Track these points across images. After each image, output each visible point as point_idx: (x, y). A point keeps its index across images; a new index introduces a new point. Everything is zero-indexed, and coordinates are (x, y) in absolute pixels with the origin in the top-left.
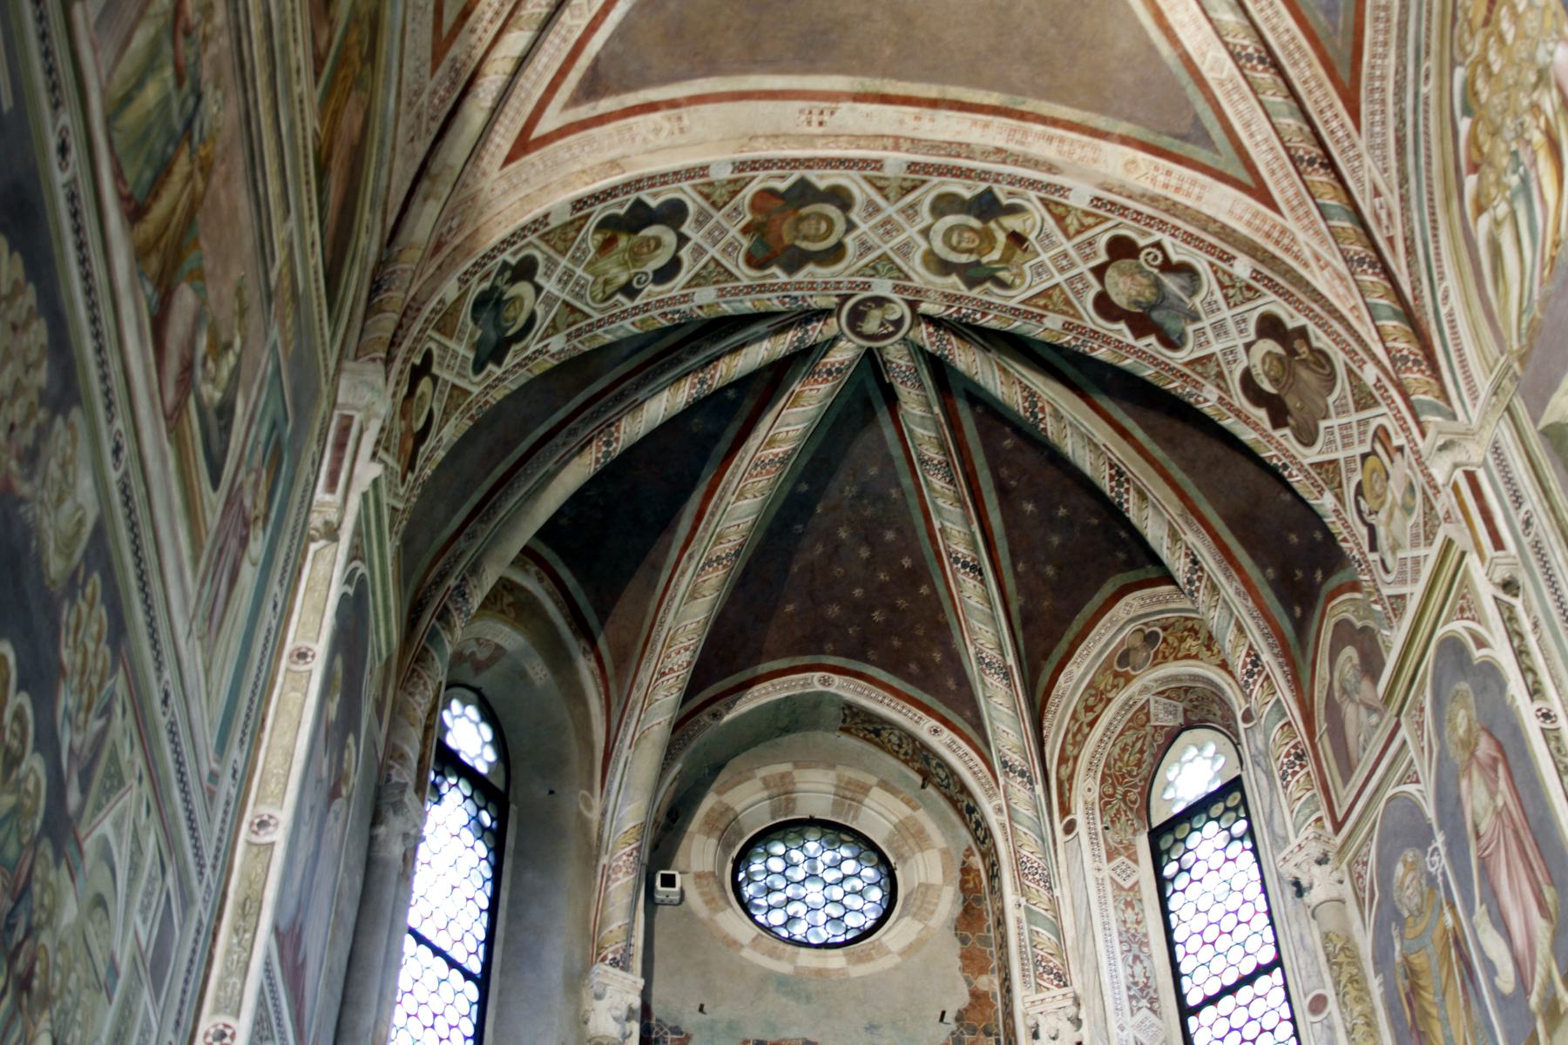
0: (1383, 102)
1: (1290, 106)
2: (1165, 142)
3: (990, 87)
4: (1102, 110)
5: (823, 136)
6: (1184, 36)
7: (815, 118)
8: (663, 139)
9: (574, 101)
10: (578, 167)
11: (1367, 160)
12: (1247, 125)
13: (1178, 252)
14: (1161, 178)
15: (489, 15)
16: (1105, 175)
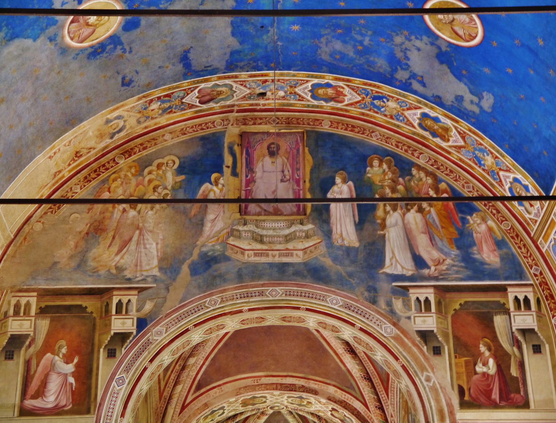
0: (394, 394)
1: (372, 391)
2: (344, 388)
3: (300, 373)
4: (328, 379)
5: (259, 385)
6: (347, 365)
7: (256, 382)
8: (217, 395)
9: (195, 392)
10: (197, 408)
11: (390, 407)
12: (363, 389)
13: (347, 415)
14: (343, 396)
15: (172, 381)
16: (330, 393)
